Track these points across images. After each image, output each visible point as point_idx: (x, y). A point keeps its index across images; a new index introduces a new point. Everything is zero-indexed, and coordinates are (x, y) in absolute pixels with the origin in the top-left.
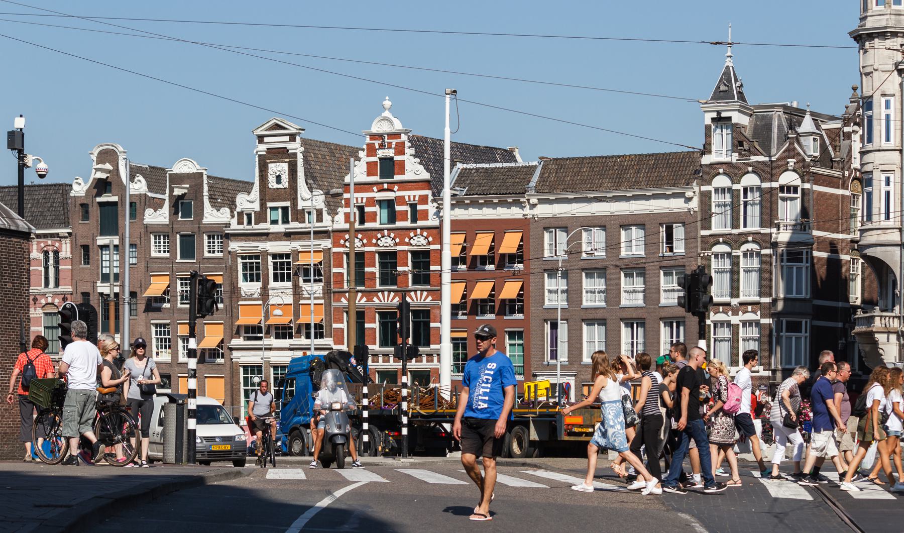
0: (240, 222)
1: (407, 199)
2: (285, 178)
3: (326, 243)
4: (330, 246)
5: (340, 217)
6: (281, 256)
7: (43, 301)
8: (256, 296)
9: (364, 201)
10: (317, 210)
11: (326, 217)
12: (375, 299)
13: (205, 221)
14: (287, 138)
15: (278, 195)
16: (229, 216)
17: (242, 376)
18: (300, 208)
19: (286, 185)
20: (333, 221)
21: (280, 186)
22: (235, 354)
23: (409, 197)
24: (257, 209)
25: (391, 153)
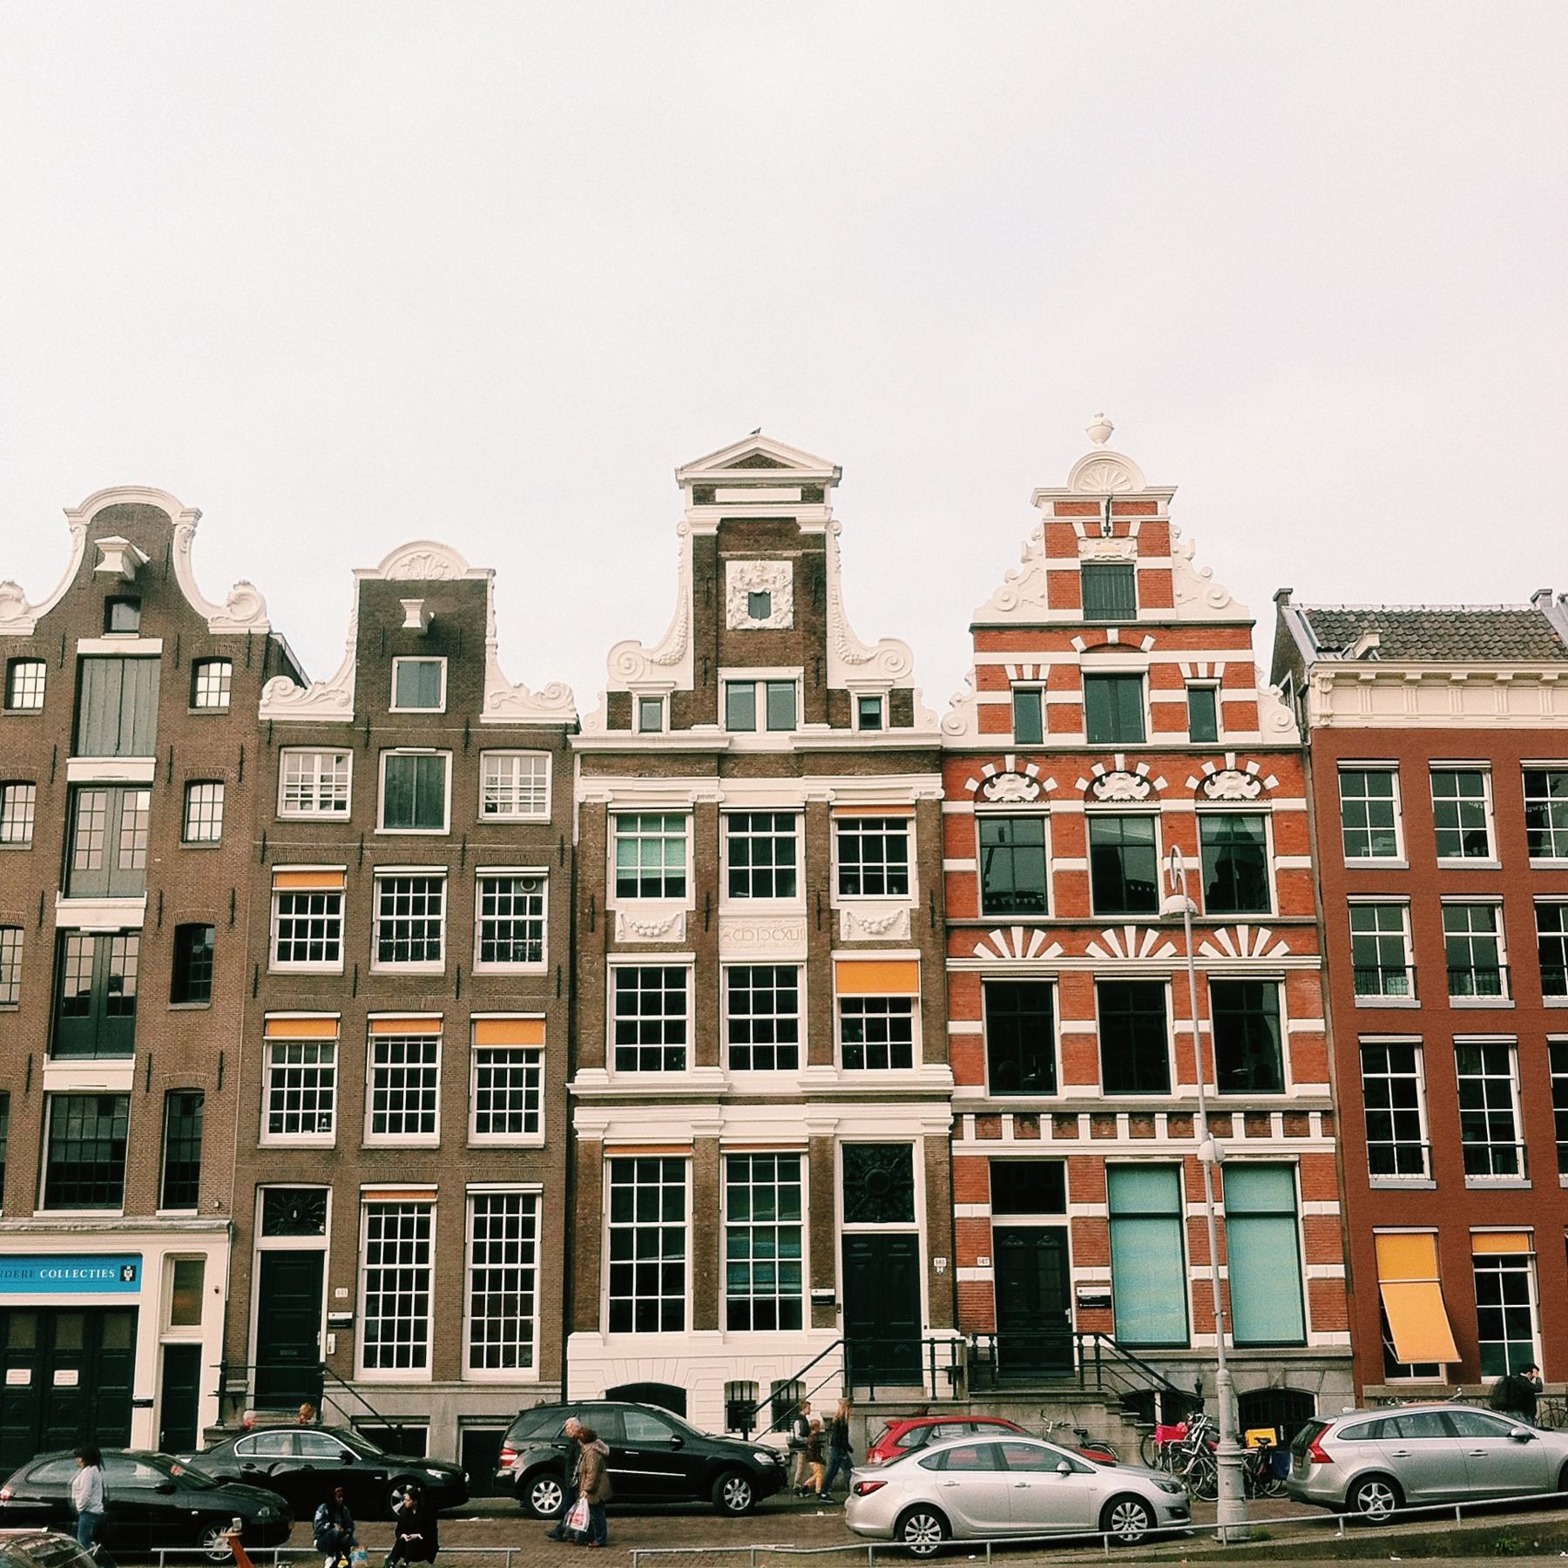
1: (1186, 672)
3: (929, 785)
4: (941, 794)
6: (762, 820)
9: (1044, 673)
10: (893, 694)
12: (1093, 949)
15: (762, 647)
17: (608, 1185)
18: (835, 682)
19: (788, 621)
23: (1194, 666)
24: (686, 682)
25: (1124, 550)
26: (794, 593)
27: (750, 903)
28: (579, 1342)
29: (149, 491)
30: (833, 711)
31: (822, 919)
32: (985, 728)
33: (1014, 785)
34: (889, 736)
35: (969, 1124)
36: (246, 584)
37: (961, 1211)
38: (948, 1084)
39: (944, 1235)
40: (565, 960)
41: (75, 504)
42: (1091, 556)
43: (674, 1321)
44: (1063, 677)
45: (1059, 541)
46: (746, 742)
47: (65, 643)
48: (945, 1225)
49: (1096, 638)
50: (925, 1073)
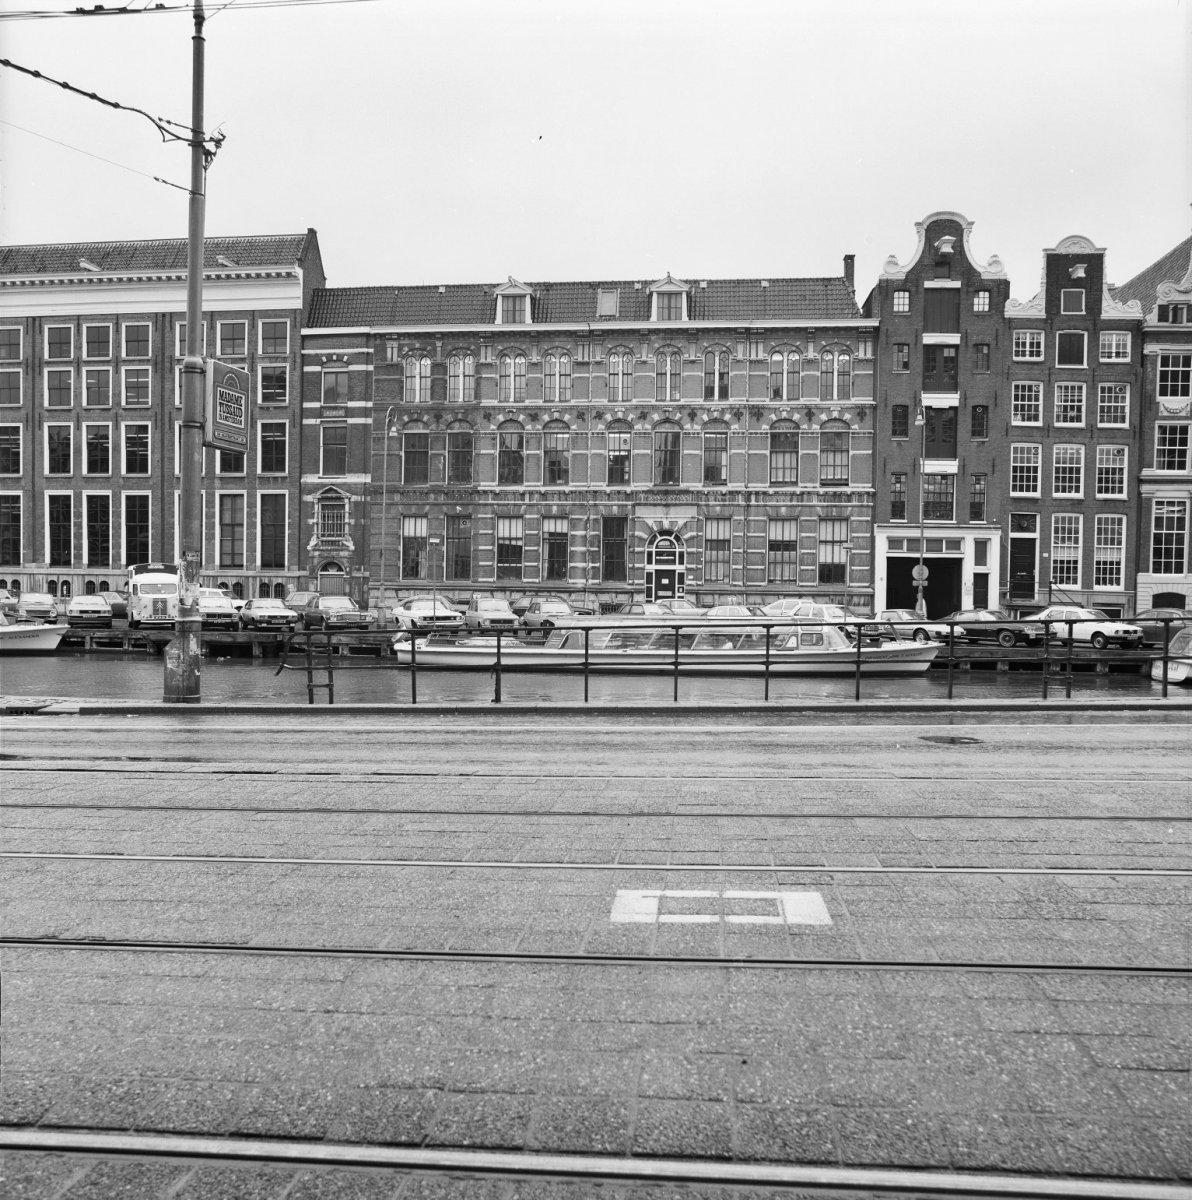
0: (1163, 317)
8: (1183, 414)
13: (1104, 316)
22: (1145, 488)
28: (1142, 577)
29: (953, 214)
36: (995, 256)
40: (1137, 423)
43: (1179, 570)
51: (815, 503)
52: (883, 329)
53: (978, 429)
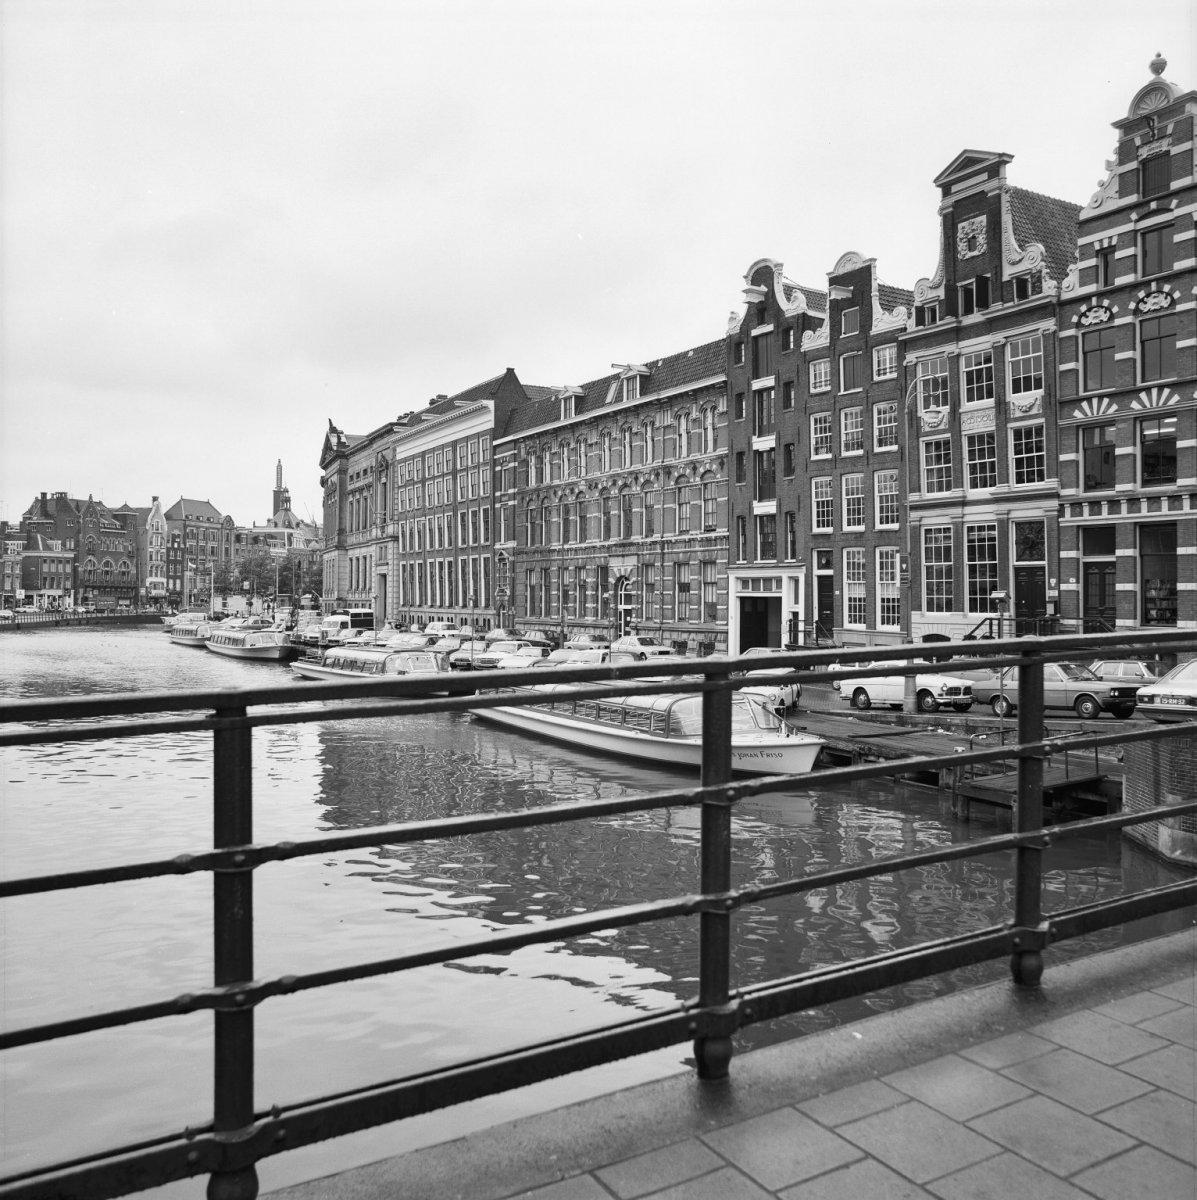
0: (920, 321)
2: (981, 239)
3: (1049, 324)
5: (1072, 279)
7: (702, 470)
8: (942, 427)
11: (1049, 287)
13: (874, 331)
14: (985, 176)
16: (906, 317)
18: (1006, 278)
20: (1059, 288)
21: (976, 253)
26: (987, 232)
27: (976, 404)
28: (915, 616)
30: (1005, 293)
31: (1002, 407)
32: (1082, 284)
33: (1097, 314)
34: (1034, 300)
35: (1068, 511)
37: (1064, 554)
38: (1054, 489)
39: (1055, 568)
41: (745, 274)
42: (1144, 156)
44: (1130, 238)
45: (1125, 152)
46: (968, 320)
47: (748, 333)
48: (1055, 561)
49: (1144, 210)
50: (1050, 483)
51: (697, 548)
52: (729, 382)
53: (789, 470)
